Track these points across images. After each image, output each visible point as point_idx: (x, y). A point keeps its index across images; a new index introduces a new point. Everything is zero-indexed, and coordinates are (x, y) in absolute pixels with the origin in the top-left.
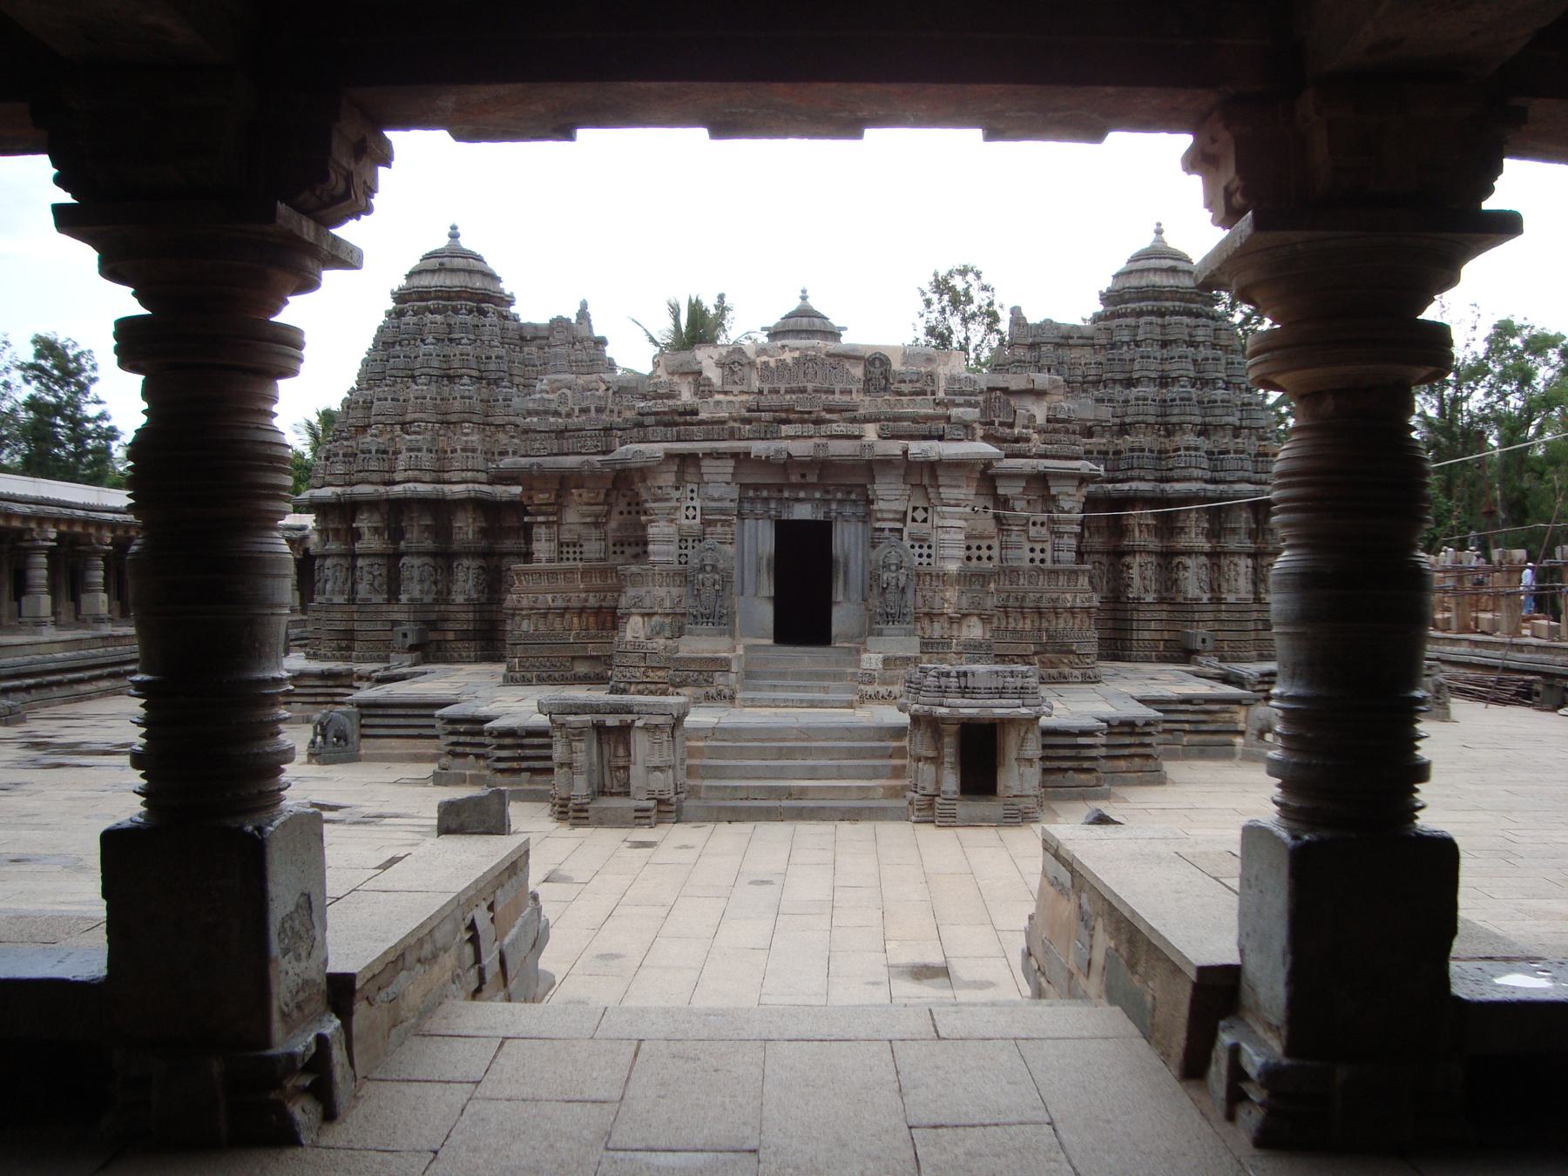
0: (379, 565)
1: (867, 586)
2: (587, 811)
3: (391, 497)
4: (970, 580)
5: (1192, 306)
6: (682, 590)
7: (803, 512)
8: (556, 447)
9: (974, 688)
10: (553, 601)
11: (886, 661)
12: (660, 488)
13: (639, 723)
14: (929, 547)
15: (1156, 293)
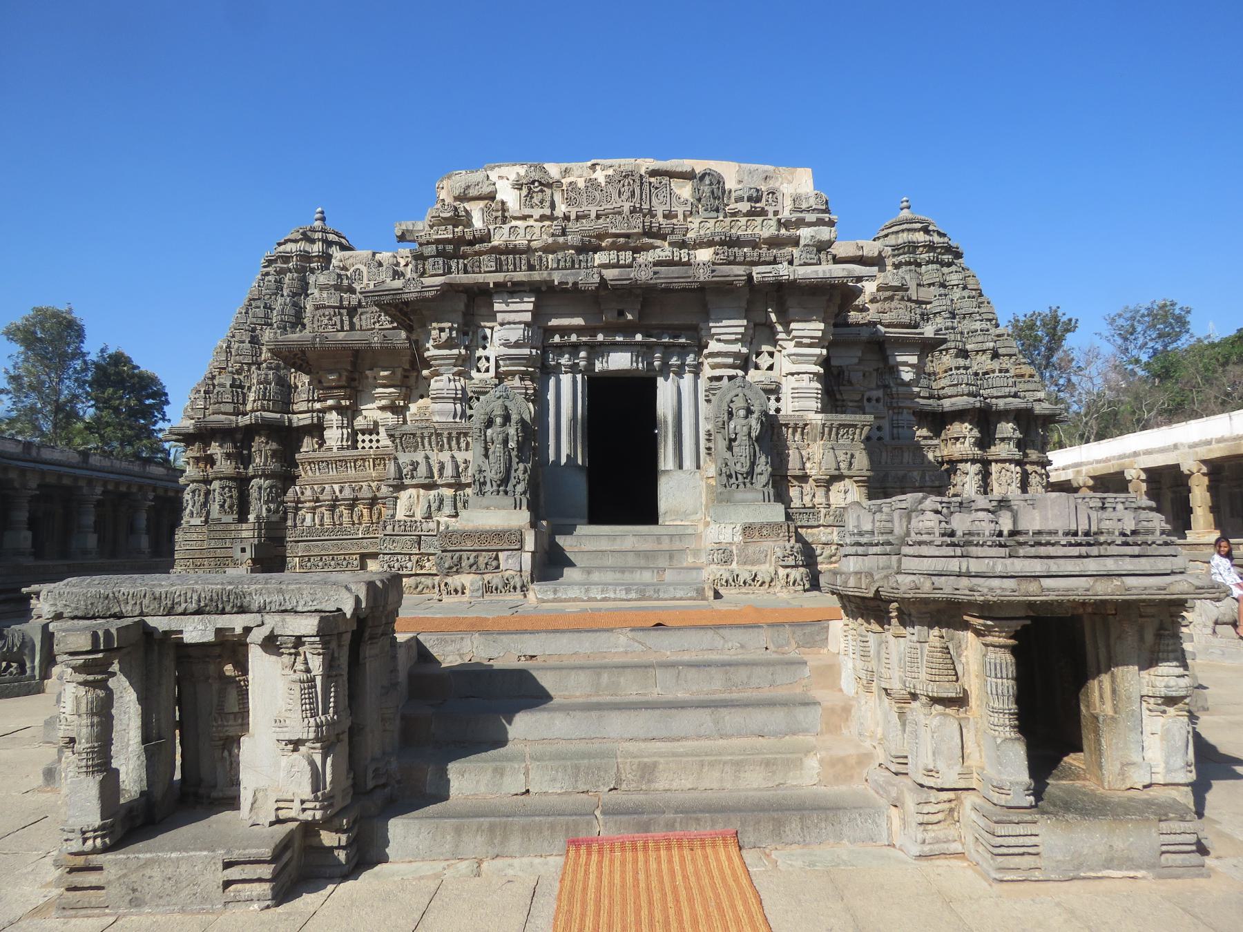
0: (230, 488)
1: (703, 451)
2: (100, 869)
3: (240, 424)
4: (837, 434)
5: (944, 257)
6: (469, 455)
7: (620, 361)
8: (346, 323)
9: (1039, 533)
10: (341, 491)
11: (748, 529)
12: (442, 330)
13: (264, 632)
14: (778, 400)
15: (912, 247)
